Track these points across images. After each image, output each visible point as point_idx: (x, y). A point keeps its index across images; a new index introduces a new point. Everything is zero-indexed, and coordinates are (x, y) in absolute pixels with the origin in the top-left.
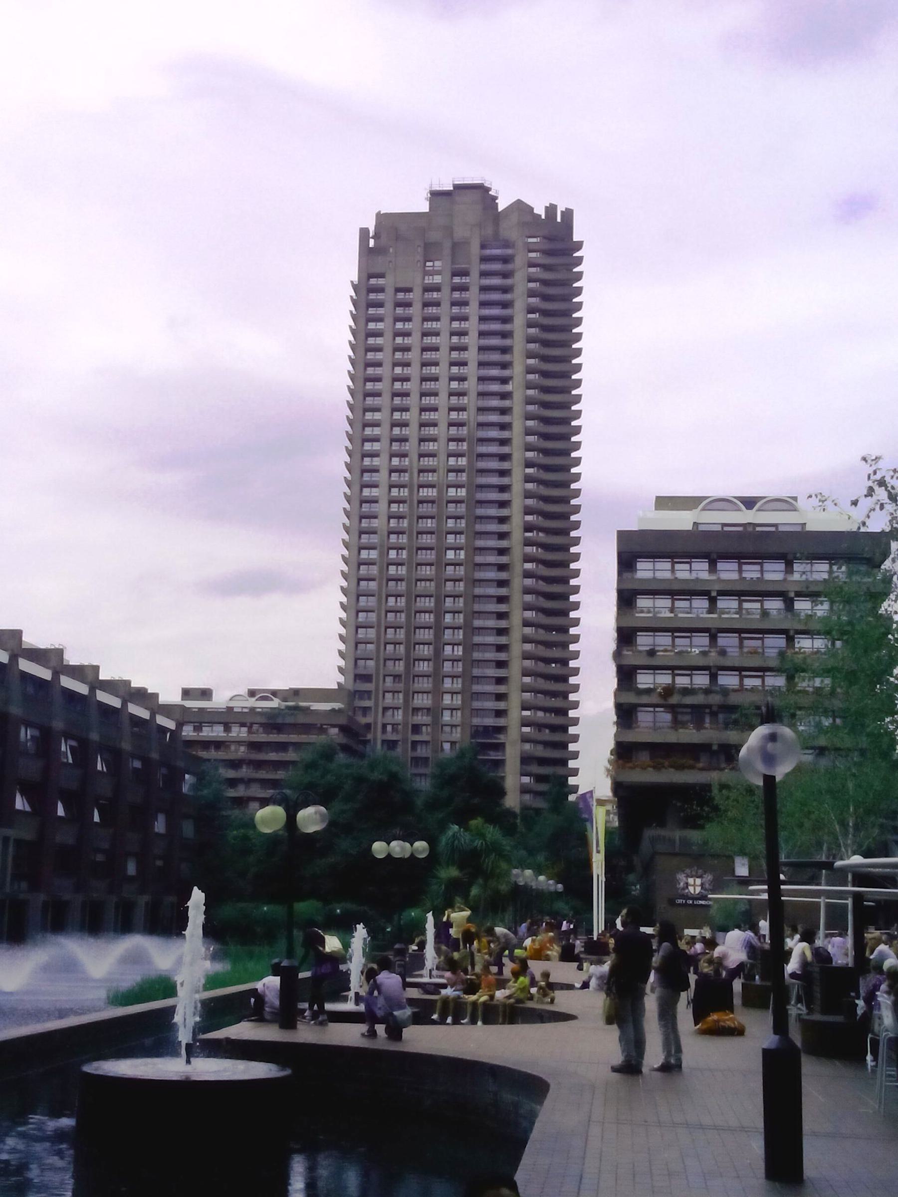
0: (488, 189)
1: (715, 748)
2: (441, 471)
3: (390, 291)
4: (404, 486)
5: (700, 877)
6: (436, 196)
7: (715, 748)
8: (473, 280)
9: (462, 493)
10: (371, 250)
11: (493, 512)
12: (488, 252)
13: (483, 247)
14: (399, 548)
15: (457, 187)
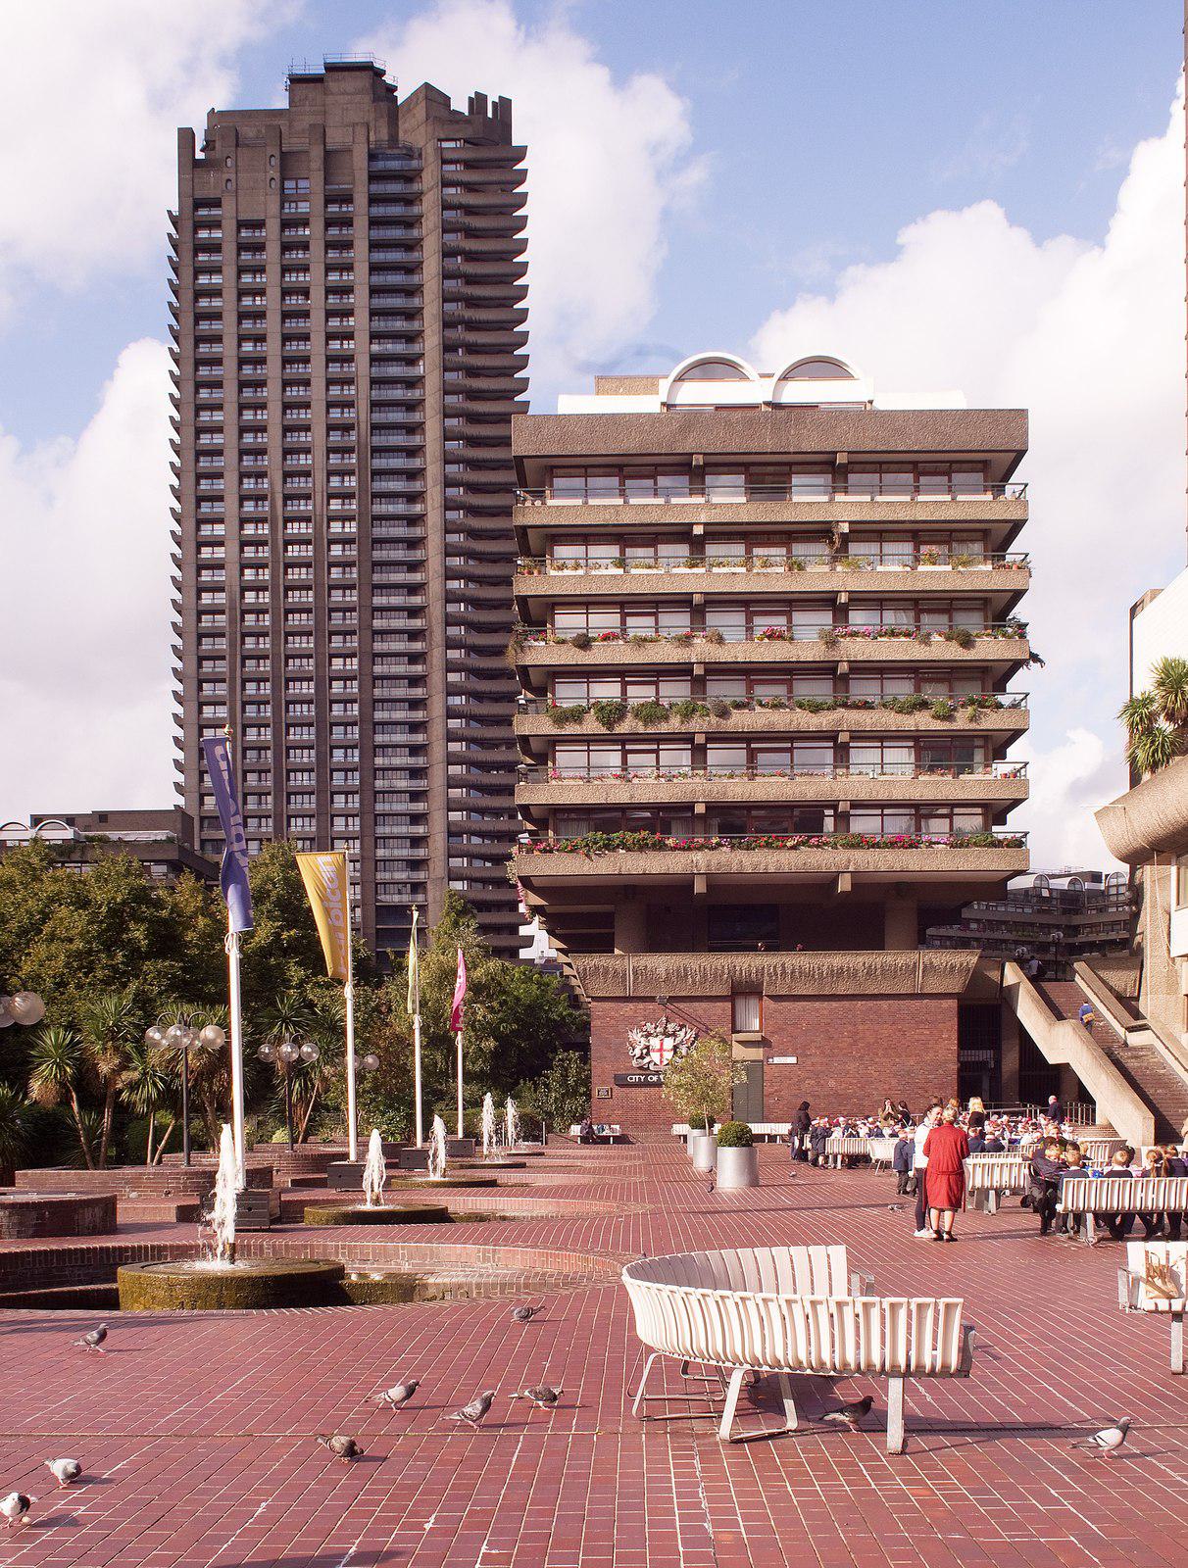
0: (380, 73)
1: (700, 809)
2: (318, 498)
3: (230, 225)
4: (263, 521)
5: (674, 1035)
6: (298, 81)
7: (700, 809)
8: (360, 209)
9: (351, 528)
10: (197, 163)
11: (399, 554)
12: (380, 165)
13: (372, 157)
14: (259, 611)
15: (331, 68)
